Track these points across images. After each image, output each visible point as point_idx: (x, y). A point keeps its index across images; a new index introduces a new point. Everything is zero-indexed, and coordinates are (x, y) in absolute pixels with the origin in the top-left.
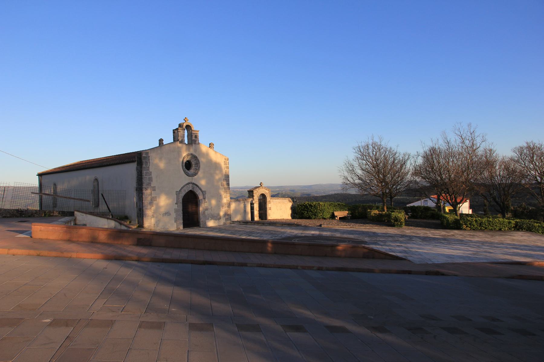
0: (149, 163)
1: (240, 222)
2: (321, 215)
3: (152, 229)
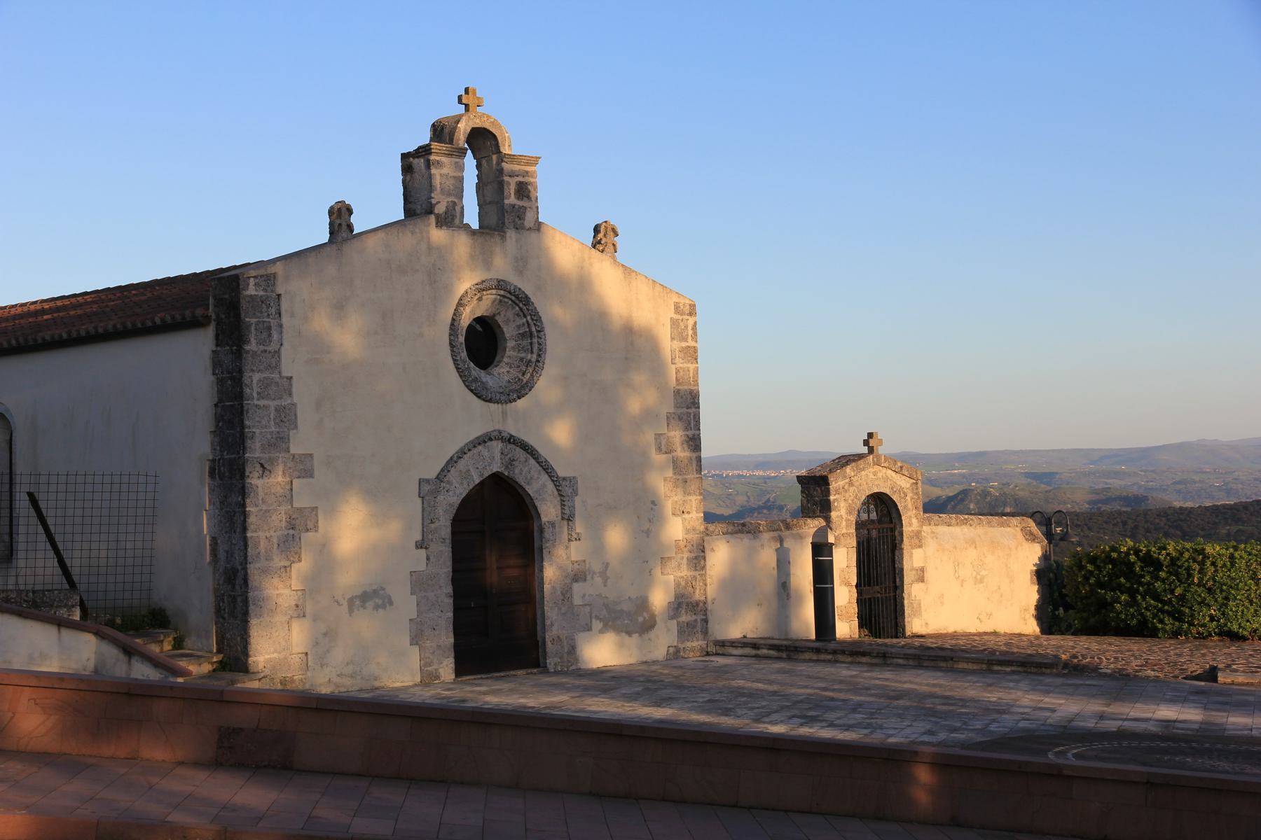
1: (755, 646)
2: (1212, 618)
3: (293, 681)
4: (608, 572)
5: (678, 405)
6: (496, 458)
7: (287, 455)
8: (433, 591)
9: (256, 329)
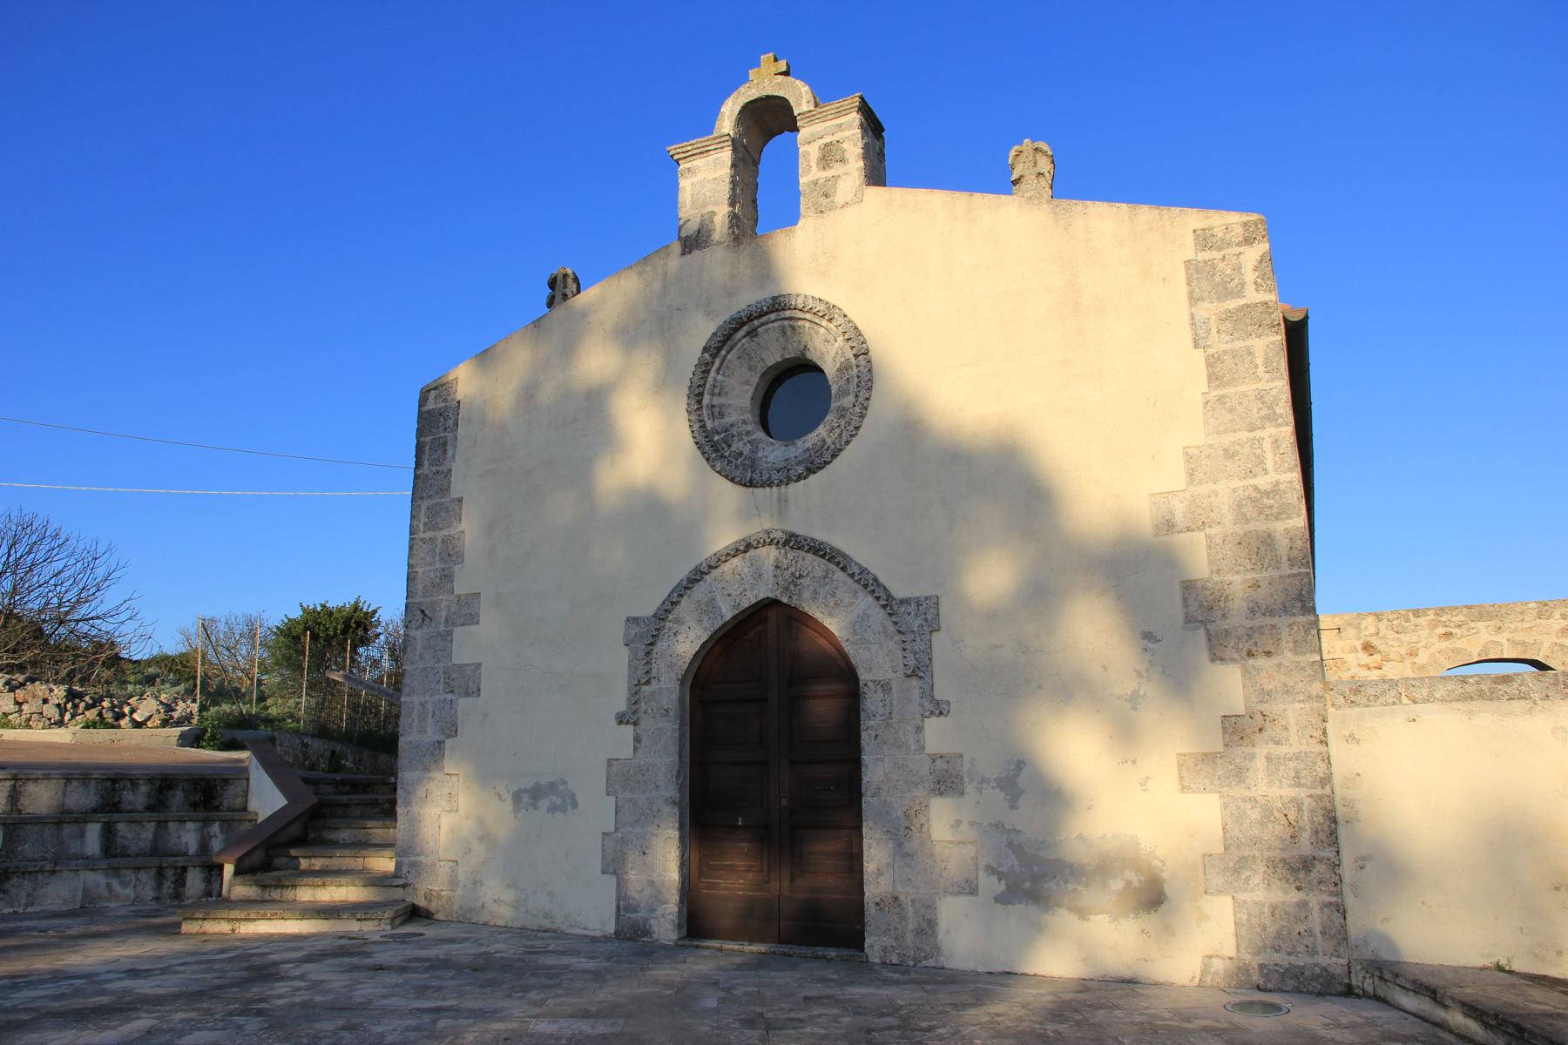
3: (439, 897)
4: (1019, 779)
5: (1221, 429)
6: (765, 575)
7: (451, 598)
8: (644, 792)
9: (430, 449)
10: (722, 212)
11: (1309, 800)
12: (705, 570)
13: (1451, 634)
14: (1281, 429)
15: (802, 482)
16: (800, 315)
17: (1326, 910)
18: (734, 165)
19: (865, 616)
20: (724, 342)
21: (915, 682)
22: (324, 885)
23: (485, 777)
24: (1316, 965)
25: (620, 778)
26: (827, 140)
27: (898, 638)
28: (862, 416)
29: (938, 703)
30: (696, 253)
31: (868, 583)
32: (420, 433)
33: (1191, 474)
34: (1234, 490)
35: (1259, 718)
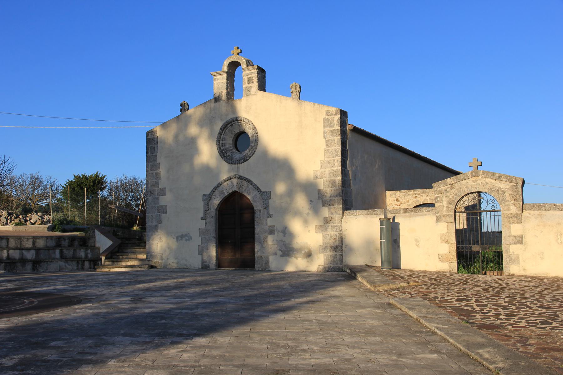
0: (157, 149)
3: (158, 263)
7: (158, 189)
9: (150, 149)
10: (224, 92)
11: (338, 235)
12: (221, 184)
13: (416, 197)
14: (339, 158)
15: (243, 164)
16: (243, 122)
17: (340, 256)
18: (227, 79)
19: (256, 195)
20: (225, 128)
21: (266, 210)
22: (128, 261)
23: (168, 234)
24: (338, 266)
25: (202, 232)
26: (249, 76)
27: (262, 200)
28: (256, 149)
29: (270, 215)
30: (218, 103)
31: (257, 188)
32: (147, 144)
33: (321, 166)
34: (329, 170)
35: (330, 218)
